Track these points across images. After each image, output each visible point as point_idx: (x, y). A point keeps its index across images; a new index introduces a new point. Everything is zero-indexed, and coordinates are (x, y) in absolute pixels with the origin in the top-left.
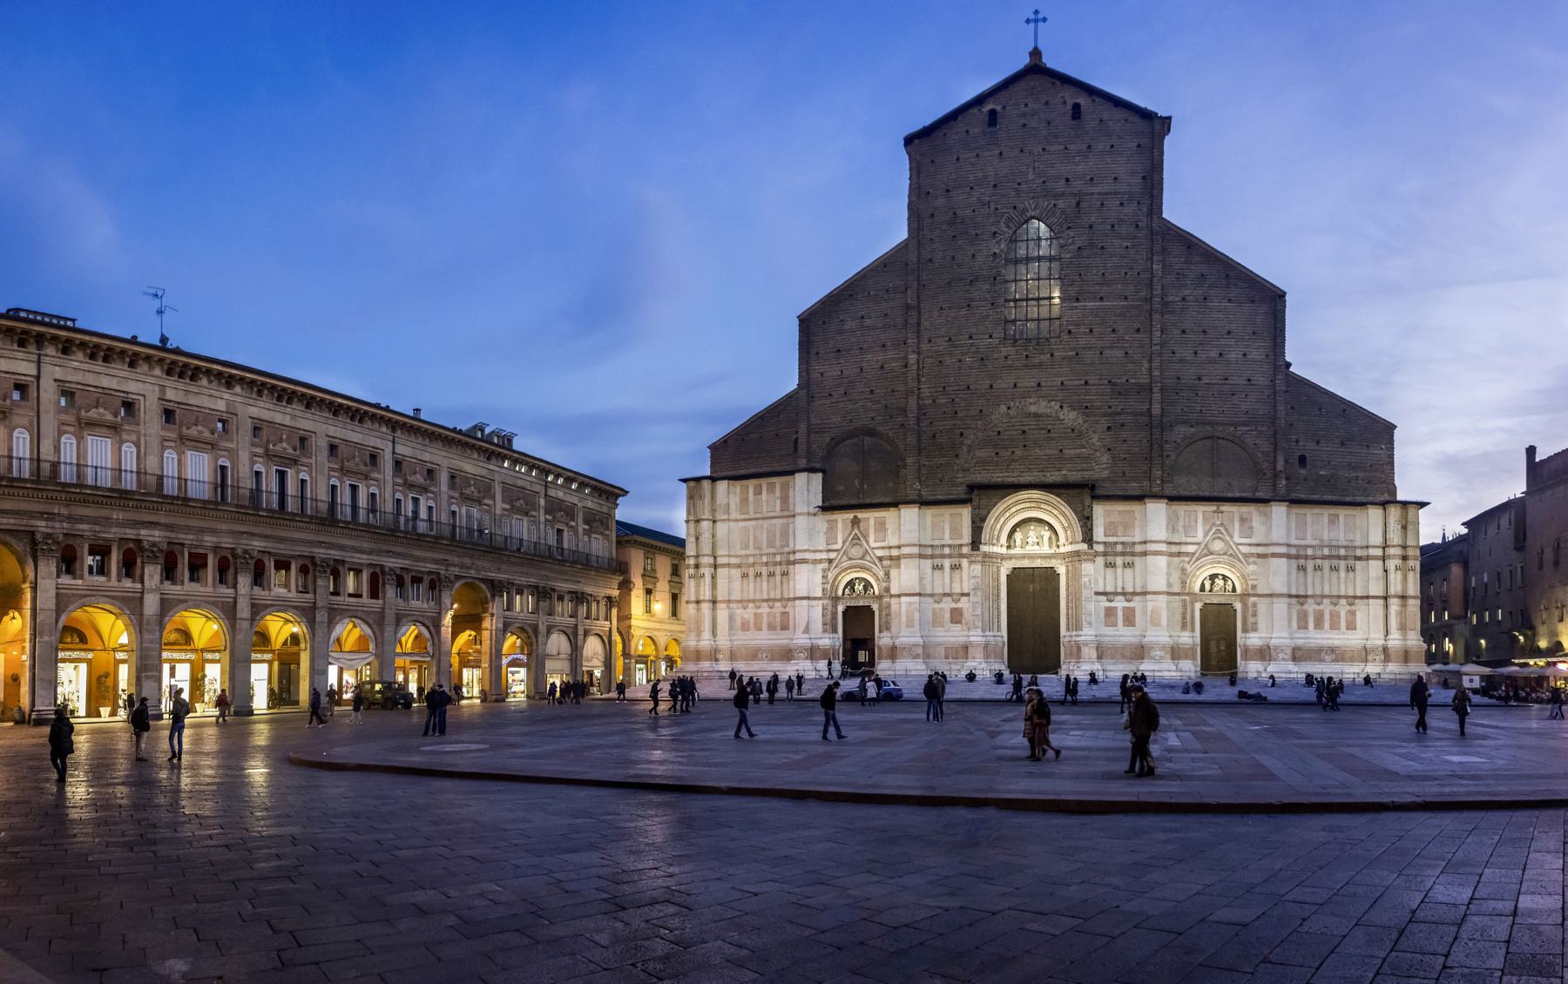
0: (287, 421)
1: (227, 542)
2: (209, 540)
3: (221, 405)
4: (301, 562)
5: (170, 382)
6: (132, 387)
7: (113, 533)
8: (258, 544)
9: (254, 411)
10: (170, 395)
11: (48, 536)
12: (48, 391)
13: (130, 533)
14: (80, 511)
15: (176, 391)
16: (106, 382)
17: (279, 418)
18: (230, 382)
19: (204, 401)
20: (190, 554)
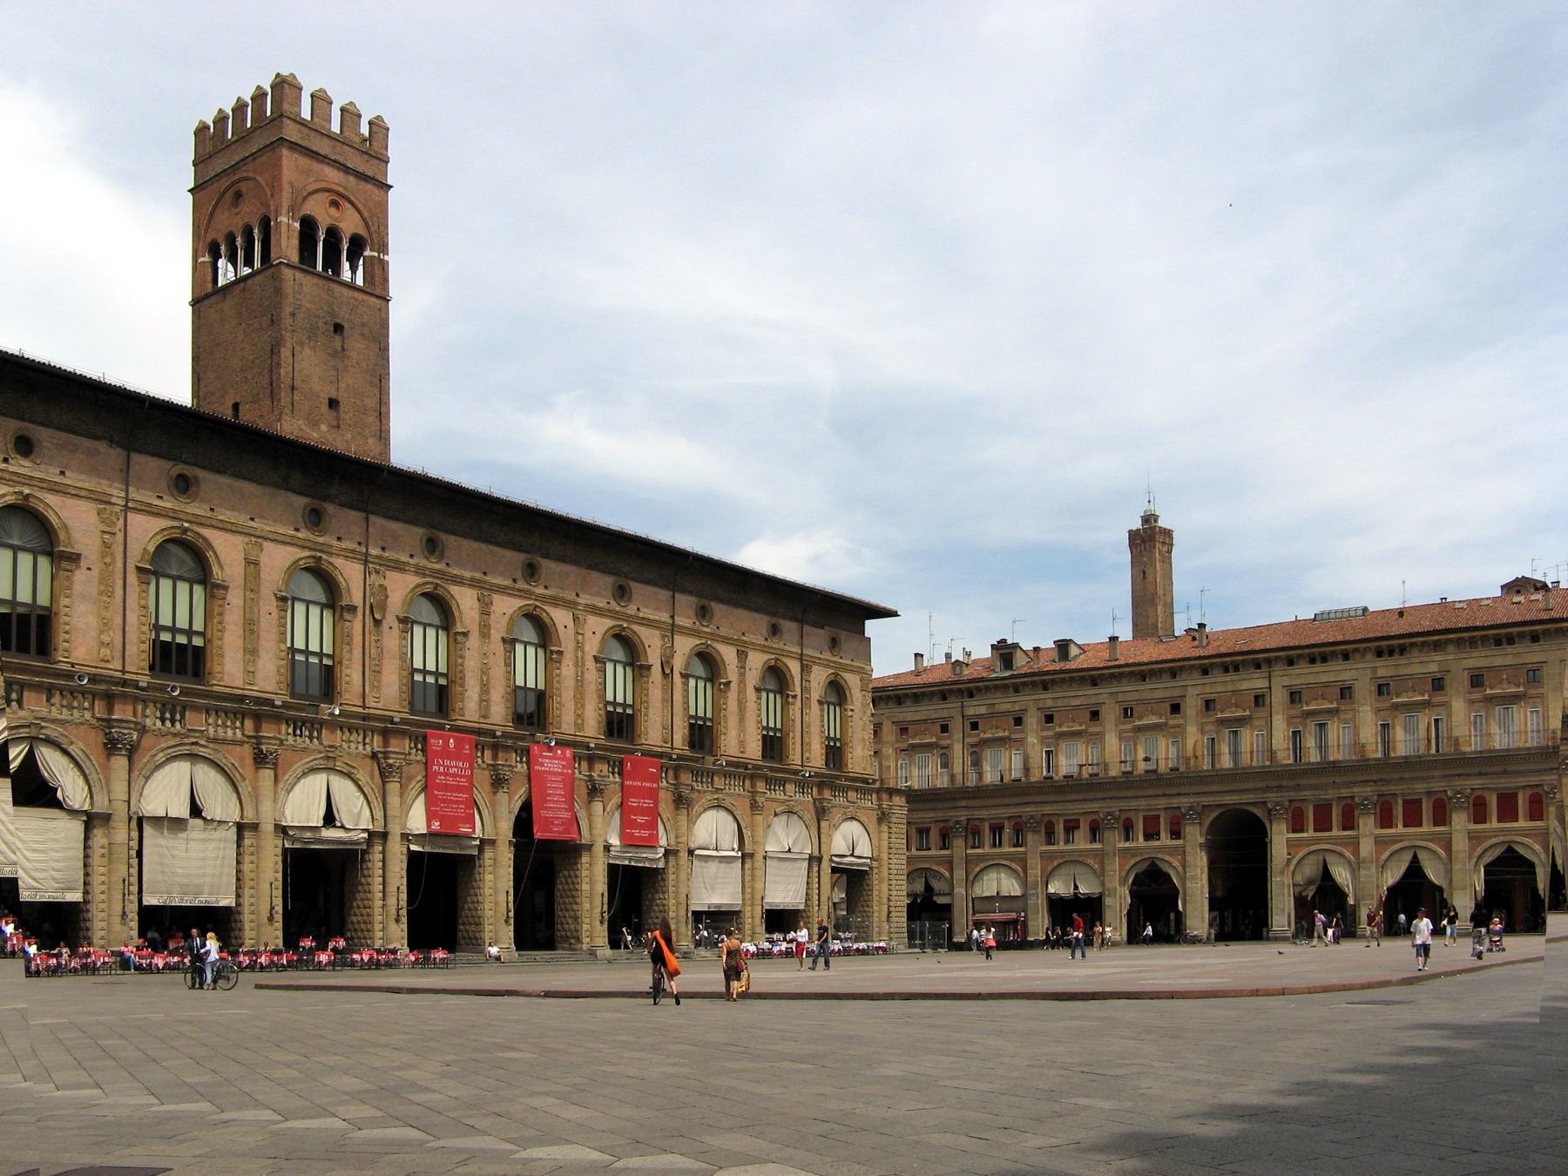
0: (1509, 661)
1: (1437, 786)
2: (1420, 787)
3: (1433, 668)
4: (1529, 792)
5: (1380, 662)
6: (1346, 676)
7: (1330, 794)
8: (1476, 782)
9: (1472, 663)
10: (1381, 672)
11: (1278, 804)
12: (1279, 697)
13: (1345, 792)
14: (1304, 781)
15: (1385, 668)
16: (1323, 678)
17: (1498, 661)
18: (1438, 646)
19: (1417, 669)
20: (1405, 802)
